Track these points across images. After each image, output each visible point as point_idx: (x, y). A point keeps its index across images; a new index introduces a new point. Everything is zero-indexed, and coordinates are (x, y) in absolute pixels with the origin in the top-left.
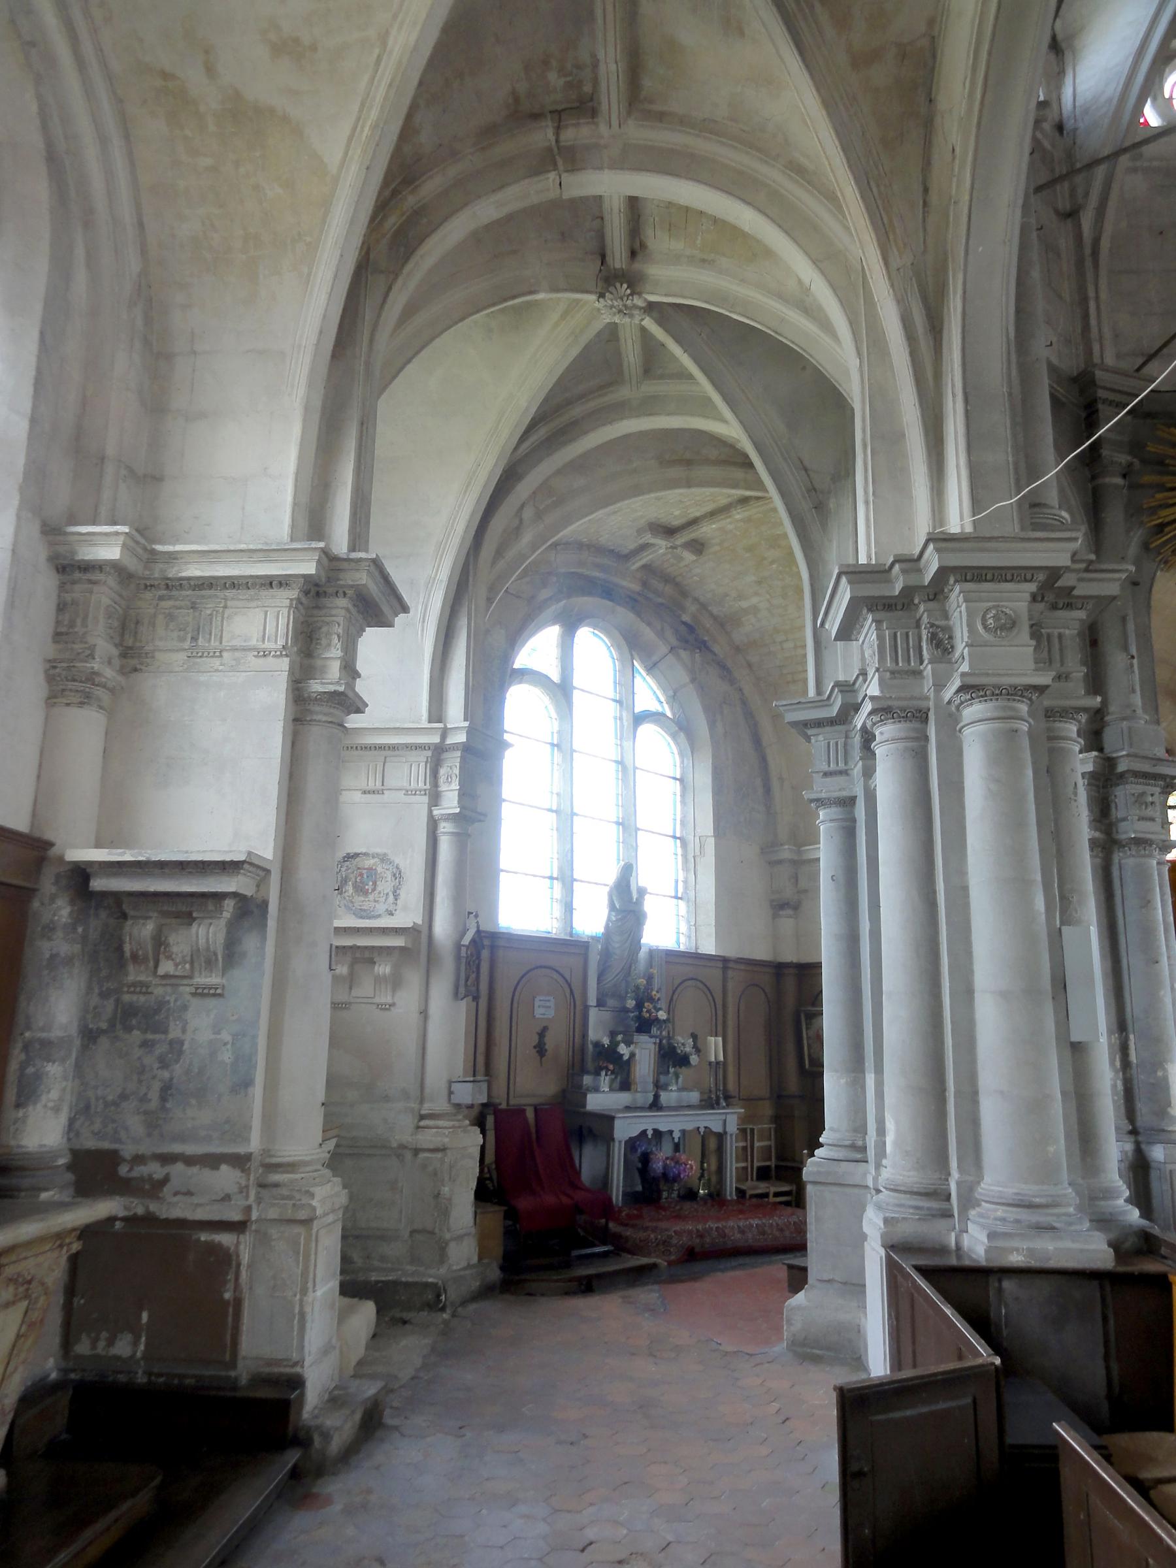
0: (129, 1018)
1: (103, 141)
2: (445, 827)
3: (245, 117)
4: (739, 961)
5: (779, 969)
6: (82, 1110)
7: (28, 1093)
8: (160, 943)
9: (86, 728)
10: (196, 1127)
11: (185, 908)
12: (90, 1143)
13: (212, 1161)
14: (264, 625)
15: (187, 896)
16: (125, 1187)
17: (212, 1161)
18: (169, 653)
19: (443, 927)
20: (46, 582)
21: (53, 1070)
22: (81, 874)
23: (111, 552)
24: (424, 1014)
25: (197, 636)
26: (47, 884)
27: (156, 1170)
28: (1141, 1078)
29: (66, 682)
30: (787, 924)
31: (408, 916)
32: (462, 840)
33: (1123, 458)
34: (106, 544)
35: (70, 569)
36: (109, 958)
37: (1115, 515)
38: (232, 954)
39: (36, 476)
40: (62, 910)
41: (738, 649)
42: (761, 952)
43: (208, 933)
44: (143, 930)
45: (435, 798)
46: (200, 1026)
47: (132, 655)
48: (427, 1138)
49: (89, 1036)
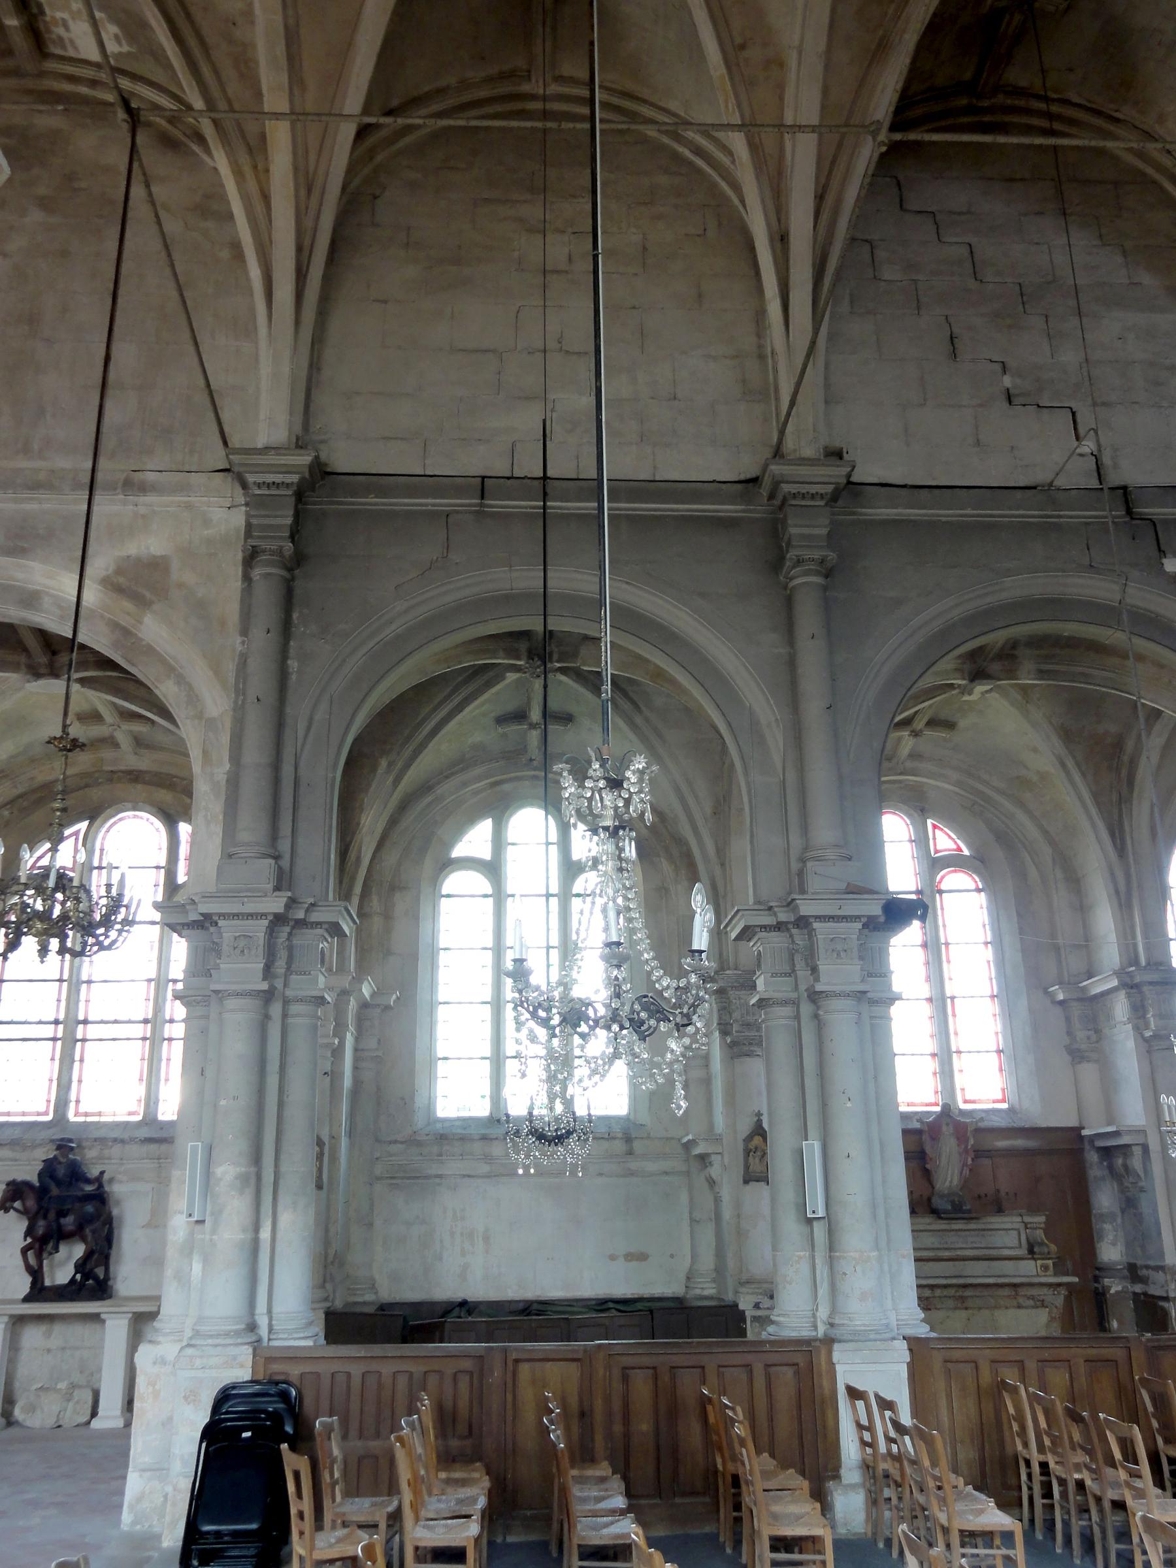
9: (1089, 1072)
29: (1077, 1055)
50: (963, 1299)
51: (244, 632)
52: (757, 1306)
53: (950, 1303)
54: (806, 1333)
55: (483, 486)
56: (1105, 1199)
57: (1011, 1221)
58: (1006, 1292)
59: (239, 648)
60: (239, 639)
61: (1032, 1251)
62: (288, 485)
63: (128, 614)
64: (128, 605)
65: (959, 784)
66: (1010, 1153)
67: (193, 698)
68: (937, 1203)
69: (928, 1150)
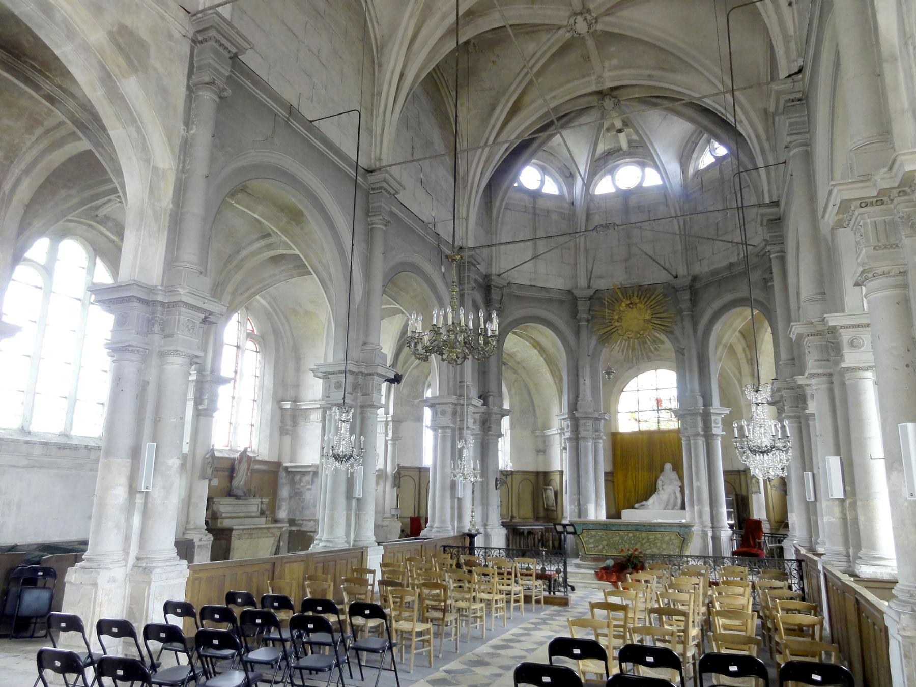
0: (296, 494)
1: (283, 324)
2: (389, 442)
3: (307, 313)
4: (518, 472)
5: (537, 474)
6: (290, 511)
7: (280, 508)
8: (301, 480)
9: (287, 439)
10: (307, 514)
11: (304, 474)
12: (291, 517)
13: (310, 520)
14: (316, 416)
15: (303, 472)
16: (296, 525)
17: (310, 520)
18: (302, 423)
19: (389, 469)
20: (279, 412)
21: (284, 504)
22: (286, 468)
23: (288, 406)
24: (384, 491)
25: (306, 418)
26: (281, 470)
27: (301, 522)
28: (583, 509)
29: (283, 431)
30: (541, 457)
31: (380, 465)
32: (394, 445)
33: (585, 316)
34: (287, 405)
35: (282, 409)
36: (292, 483)
37: (584, 334)
38: (313, 482)
39: (275, 393)
40: (284, 474)
41: (518, 363)
42: (531, 468)
43: (308, 478)
44: (297, 478)
45: (387, 435)
46: (308, 496)
47: (295, 424)
48: (385, 523)
49: (290, 497)
50: (251, 534)
51: (187, 124)
52: (201, 540)
53: (247, 536)
54: (346, 546)
55: (291, 110)
56: (284, 492)
57: (257, 500)
58: (265, 531)
59: (182, 132)
60: (182, 127)
61: (262, 513)
62: (229, 52)
63: (119, 67)
64: (122, 61)
65: (269, 303)
66: (258, 471)
67: (144, 149)
68: (236, 491)
69: (237, 467)
